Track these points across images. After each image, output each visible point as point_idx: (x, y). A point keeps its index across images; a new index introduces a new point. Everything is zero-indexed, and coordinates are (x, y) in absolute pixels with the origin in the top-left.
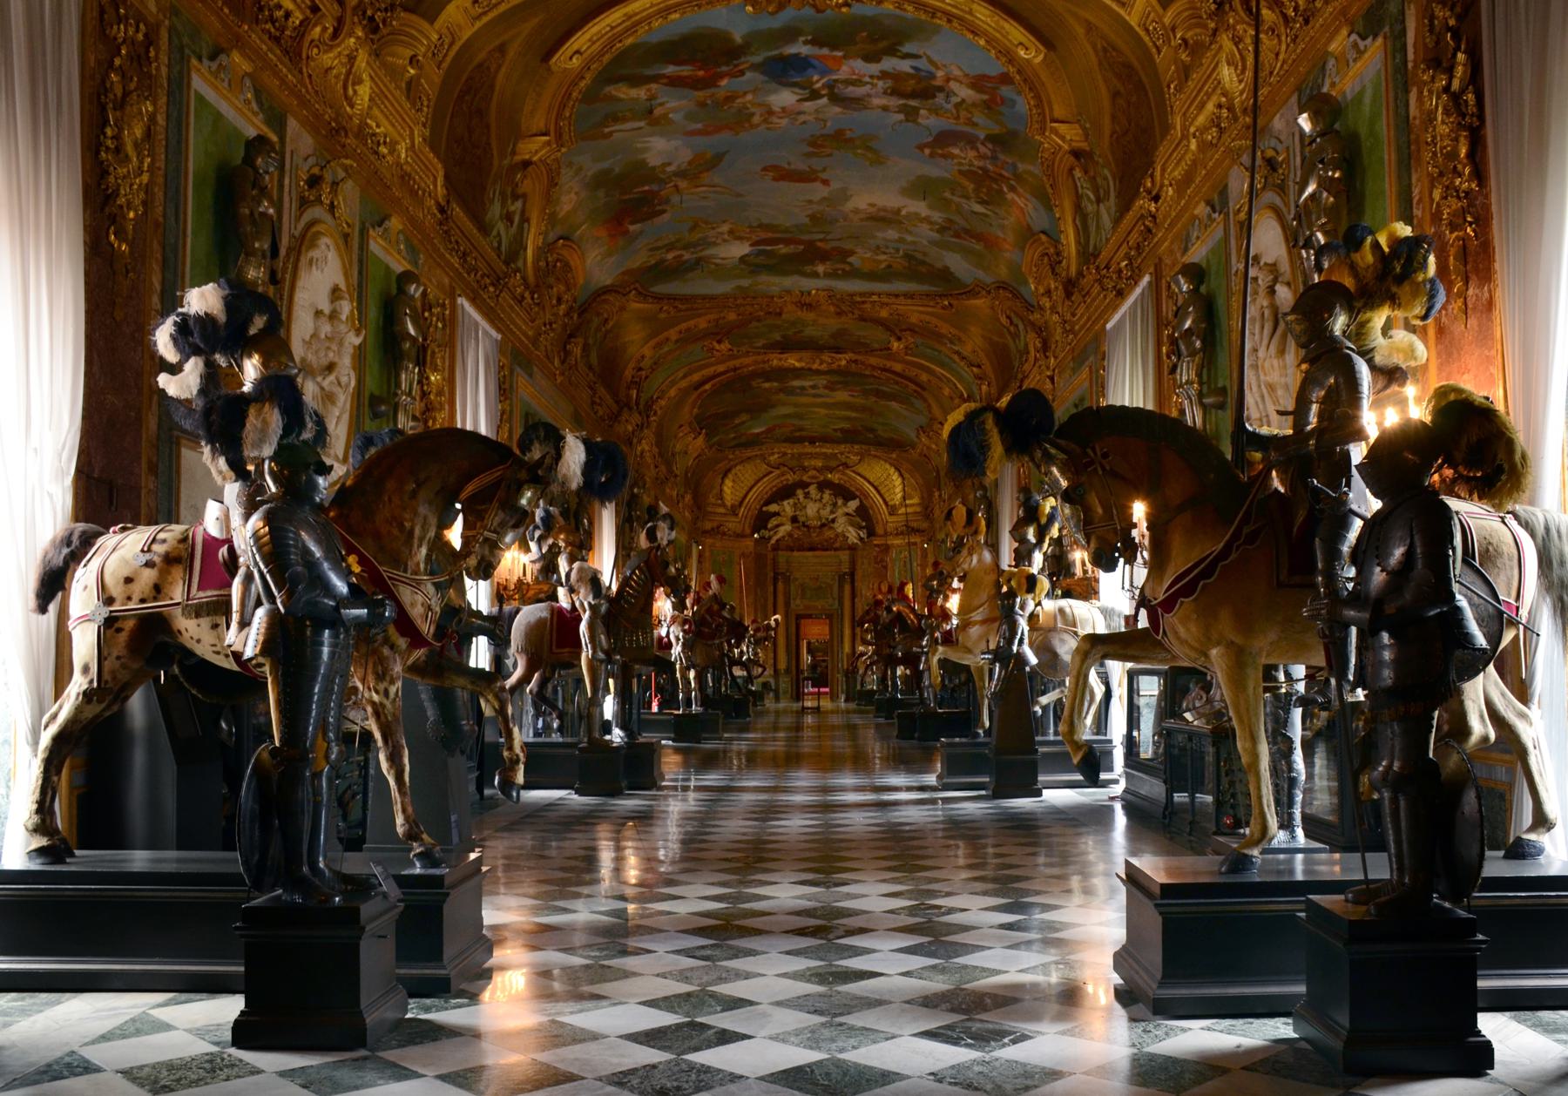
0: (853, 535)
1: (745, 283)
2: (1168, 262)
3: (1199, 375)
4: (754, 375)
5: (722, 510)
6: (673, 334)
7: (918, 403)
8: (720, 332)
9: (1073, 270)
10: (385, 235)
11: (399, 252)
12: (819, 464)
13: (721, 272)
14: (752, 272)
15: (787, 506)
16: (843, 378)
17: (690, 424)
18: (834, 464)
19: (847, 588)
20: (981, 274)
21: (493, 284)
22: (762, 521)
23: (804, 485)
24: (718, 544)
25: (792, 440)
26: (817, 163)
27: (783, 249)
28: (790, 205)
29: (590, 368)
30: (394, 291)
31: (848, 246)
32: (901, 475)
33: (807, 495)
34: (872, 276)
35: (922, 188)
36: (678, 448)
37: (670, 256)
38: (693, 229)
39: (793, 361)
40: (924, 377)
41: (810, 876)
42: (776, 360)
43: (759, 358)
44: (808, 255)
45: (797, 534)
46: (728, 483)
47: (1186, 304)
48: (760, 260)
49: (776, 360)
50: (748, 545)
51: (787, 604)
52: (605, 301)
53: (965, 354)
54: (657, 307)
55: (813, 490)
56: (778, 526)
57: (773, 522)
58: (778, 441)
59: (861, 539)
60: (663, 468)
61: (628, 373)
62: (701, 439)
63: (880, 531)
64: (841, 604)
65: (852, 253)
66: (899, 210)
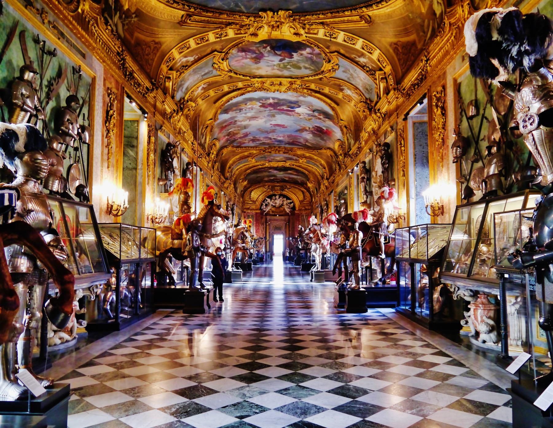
1: (302, 98)
13: (309, 105)
14: (298, 102)
20: (218, 121)
26: (273, 128)
27: (285, 108)
28: (281, 119)
31: (262, 109)
34: (251, 99)
35: (245, 127)
37: (321, 117)
38: (310, 119)
44: (277, 105)
48: (293, 105)
65: (260, 106)
66: (250, 120)
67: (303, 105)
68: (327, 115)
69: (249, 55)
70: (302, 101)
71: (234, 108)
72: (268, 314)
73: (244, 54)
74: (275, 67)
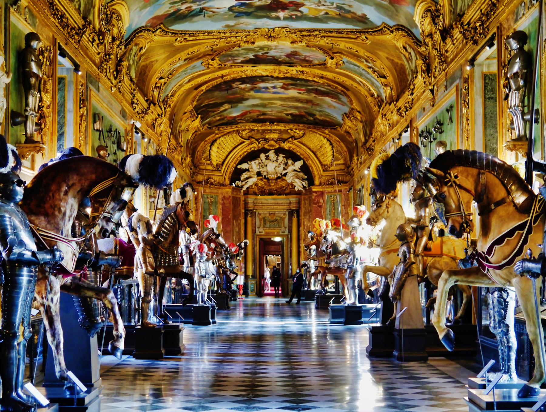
0: (299, 185)
1: (231, 23)
2: (506, 26)
3: (522, 101)
4: (234, 80)
5: (210, 168)
6: (183, 55)
7: (344, 99)
8: (213, 53)
9: (447, 22)
10: (18, 11)
11: (26, 20)
12: (276, 136)
13: (215, 15)
14: (236, 17)
15: (254, 166)
16: (294, 82)
17: (191, 112)
18: (285, 136)
19: (295, 220)
21: (76, 33)
22: (237, 174)
23: (266, 151)
24: (208, 190)
25: (257, 121)
29: (131, 80)
30: (23, 46)
32: (331, 144)
33: (267, 158)
34: (316, 19)
36: (183, 127)
37: (184, 7)
39: (261, 70)
40: (348, 82)
41: (288, 405)
42: (250, 70)
43: (239, 69)
45: (260, 183)
46: (214, 148)
47: (515, 57)
48: (243, 9)
49: (250, 70)
50: (228, 191)
51: (254, 232)
52: (141, 36)
53: (376, 69)
54: (174, 39)
55: (272, 154)
56: (247, 178)
57: (244, 176)
58: (248, 121)
59: (304, 187)
60: (173, 142)
61: (154, 80)
62: (198, 120)
63: (317, 182)
64: (290, 231)
65: (302, 5)
67: (225, 14)
68: (177, 17)
69: (302, 57)
70: (229, 19)
71: (349, 16)
72: (287, 390)
73: (307, 59)
74: (274, 48)
